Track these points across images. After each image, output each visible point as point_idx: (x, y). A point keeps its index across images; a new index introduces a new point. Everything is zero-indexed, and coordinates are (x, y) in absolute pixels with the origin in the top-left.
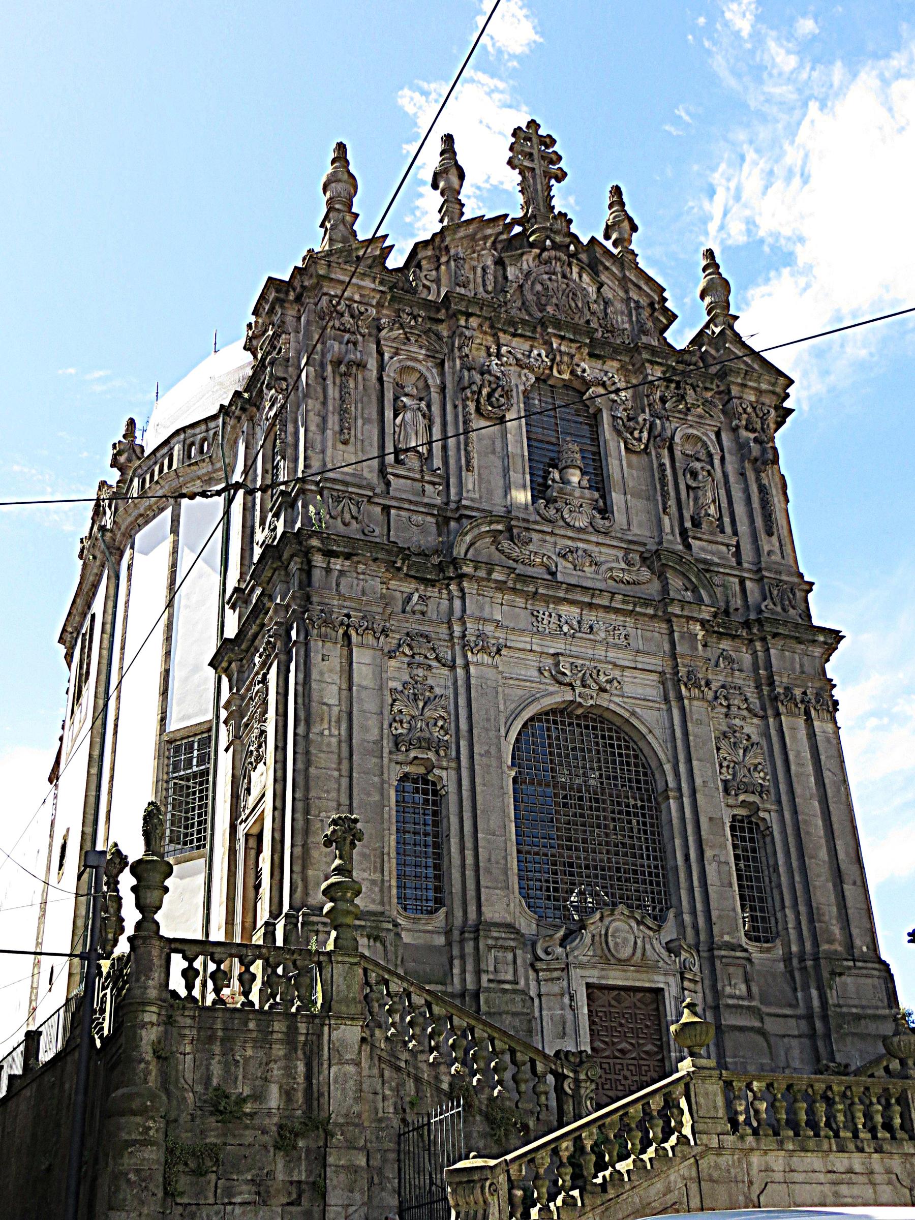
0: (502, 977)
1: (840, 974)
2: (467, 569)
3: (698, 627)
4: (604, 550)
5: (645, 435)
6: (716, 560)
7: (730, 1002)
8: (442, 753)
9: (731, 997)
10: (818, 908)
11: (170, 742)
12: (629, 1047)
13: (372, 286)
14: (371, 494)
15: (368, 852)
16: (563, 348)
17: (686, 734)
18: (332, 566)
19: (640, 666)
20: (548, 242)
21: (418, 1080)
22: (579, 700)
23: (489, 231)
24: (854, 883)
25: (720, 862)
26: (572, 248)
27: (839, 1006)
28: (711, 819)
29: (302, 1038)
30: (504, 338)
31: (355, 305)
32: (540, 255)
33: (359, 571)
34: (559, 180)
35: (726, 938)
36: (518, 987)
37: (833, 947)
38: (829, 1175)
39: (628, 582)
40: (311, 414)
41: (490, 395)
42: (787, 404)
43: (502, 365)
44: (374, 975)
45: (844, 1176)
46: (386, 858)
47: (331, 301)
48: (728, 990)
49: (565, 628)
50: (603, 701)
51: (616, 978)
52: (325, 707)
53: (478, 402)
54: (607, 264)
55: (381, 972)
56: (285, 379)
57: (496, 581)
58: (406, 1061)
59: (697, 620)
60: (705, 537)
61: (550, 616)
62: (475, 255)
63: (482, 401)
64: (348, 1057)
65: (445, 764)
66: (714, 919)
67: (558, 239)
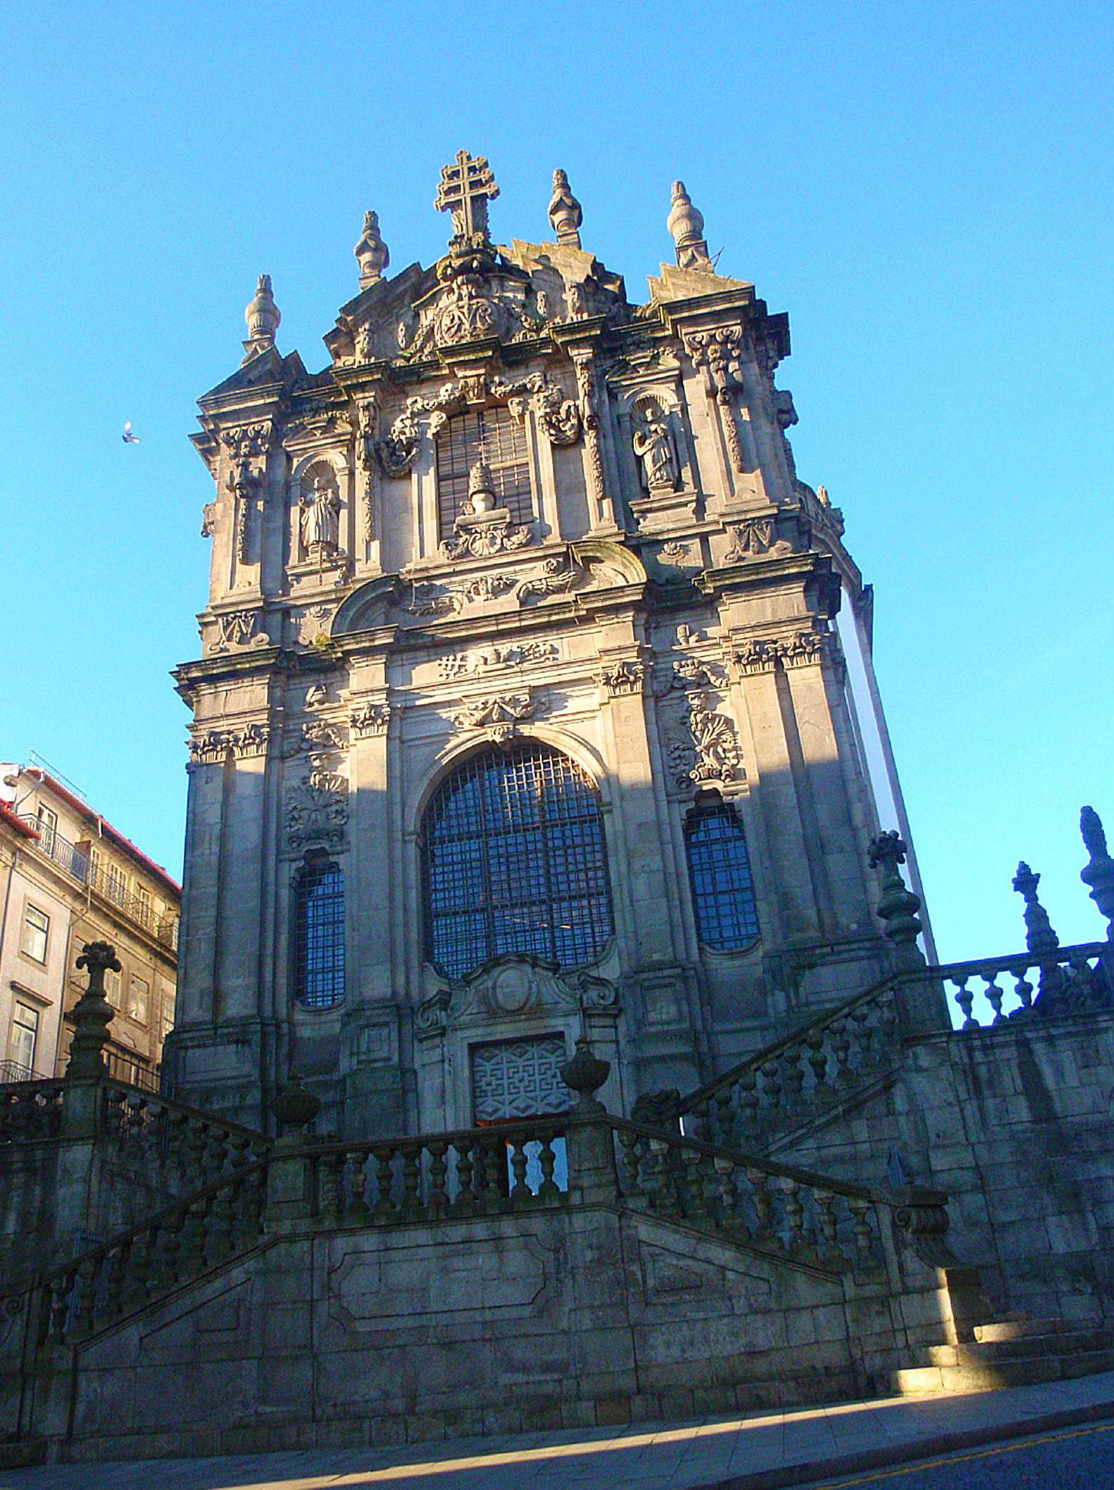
1: (811, 966)
4: (518, 568)
5: (574, 421)
6: (671, 526)
8: (335, 839)
9: (653, 1024)
12: (531, 1102)
13: (262, 402)
14: (261, 604)
19: (563, 678)
20: (449, 271)
21: (148, 1188)
22: (490, 739)
23: (401, 289)
25: (653, 872)
26: (475, 264)
27: (808, 1004)
28: (640, 826)
29: (38, 1164)
34: (493, 197)
35: (656, 956)
36: (391, 1063)
37: (805, 936)
38: (440, 1249)
41: (392, 454)
44: (112, 1092)
45: (461, 1246)
46: (269, 960)
47: (228, 434)
48: (652, 1016)
49: (470, 668)
50: (526, 730)
51: (504, 1031)
52: (206, 828)
53: (381, 465)
55: (117, 1088)
58: (135, 1172)
60: (655, 505)
62: (394, 318)
63: (386, 465)
65: (339, 848)
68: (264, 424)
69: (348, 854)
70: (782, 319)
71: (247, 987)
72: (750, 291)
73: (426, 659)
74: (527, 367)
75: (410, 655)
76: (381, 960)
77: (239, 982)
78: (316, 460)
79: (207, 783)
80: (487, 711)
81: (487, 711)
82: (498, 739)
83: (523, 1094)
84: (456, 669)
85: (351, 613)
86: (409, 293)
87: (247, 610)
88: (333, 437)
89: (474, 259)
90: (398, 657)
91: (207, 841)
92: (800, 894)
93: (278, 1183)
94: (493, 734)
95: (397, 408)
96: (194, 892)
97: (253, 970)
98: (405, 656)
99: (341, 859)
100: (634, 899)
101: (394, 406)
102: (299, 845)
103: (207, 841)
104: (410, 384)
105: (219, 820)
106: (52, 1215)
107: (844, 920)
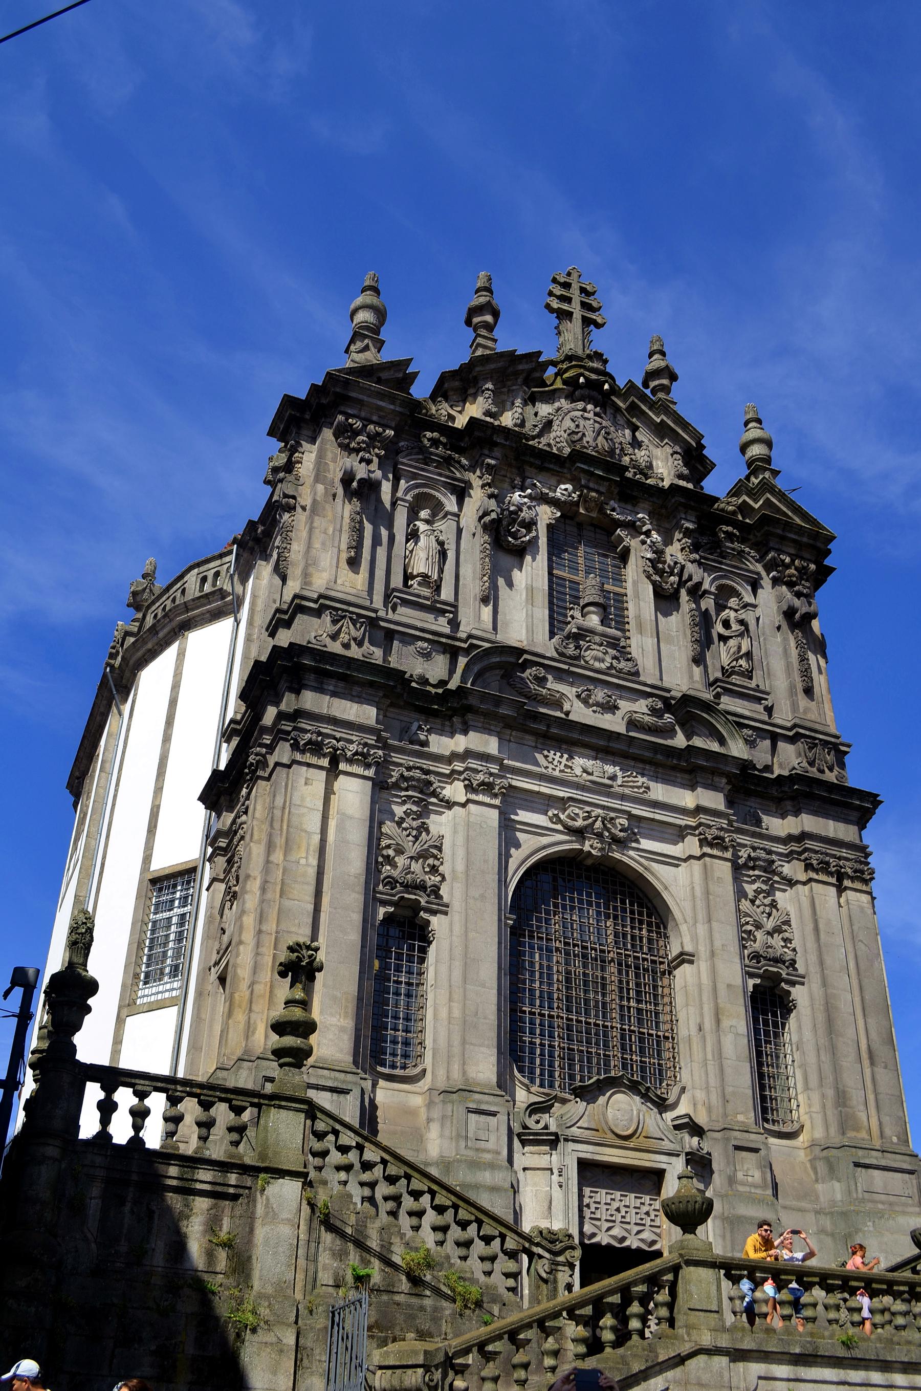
0: (482, 1145)
2: (473, 701)
3: (724, 780)
6: (747, 713)
7: (741, 1188)
9: (743, 1184)
10: (844, 1092)
11: (154, 881)
14: (373, 615)
15: (339, 995)
16: (591, 485)
17: (707, 893)
18: (326, 687)
23: (520, 367)
24: (886, 1067)
26: (606, 387)
28: (729, 986)
30: (529, 471)
31: (372, 427)
32: (574, 392)
33: (354, 693)
35: (741, 1118)
39: (650, 728)
40: (317, 531)
42: (827, 562)
43: (525, 497)
47: (347, 420)
52: (303, 834)
54: (643, 407)
56: (294, 497)
57: (504, 717)
59: (722, 774)
61: (561, 757)
62: (505, 390)
63: (502, 533)
64: (285, 1215)
66: (727, 1097)
67: (594, 376)
68: (387, 431)
69: (443, 916)
70: (830, 570)
71: (342, 1029)
72: (832, 538)
73: (533, 744)
74: (634, 505)
75: (519, 734)
76: (486, 1042)
77: (334, 1020)
78: (425, 490)
79: (306, 784)
80: (590, 820)
81: (590, 820)
82: (594, 852)
83: (647, 1227)
84: (562, 767)
85: (476, 669)
86: (524, 375)
87: (360, 616)
88: (447, 477)
89: (606, 381)
90: (508, 732)
91: (303, 849)
92: (855, 1097)
93: (693, 1289)
94: (591, 846)
95: (507, 480)
96: (287, 903)
97: (350, 1011)
98: (514, 733)
99: (436, 922)
100: (724, 1056)
101: (506, 476)
102: (392, 889)
103: (303, 849)
104: (531, 465)
105: (319, 831)
106: (250, 1257)
107: (888, 1131)
